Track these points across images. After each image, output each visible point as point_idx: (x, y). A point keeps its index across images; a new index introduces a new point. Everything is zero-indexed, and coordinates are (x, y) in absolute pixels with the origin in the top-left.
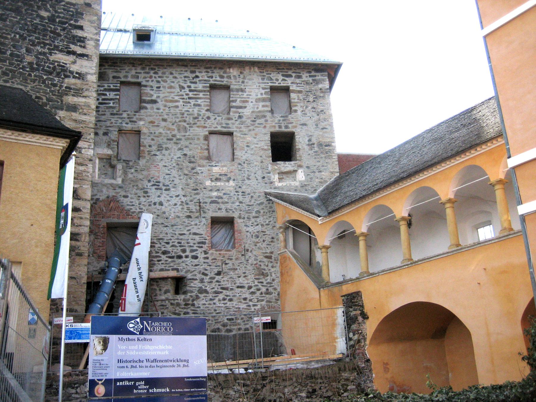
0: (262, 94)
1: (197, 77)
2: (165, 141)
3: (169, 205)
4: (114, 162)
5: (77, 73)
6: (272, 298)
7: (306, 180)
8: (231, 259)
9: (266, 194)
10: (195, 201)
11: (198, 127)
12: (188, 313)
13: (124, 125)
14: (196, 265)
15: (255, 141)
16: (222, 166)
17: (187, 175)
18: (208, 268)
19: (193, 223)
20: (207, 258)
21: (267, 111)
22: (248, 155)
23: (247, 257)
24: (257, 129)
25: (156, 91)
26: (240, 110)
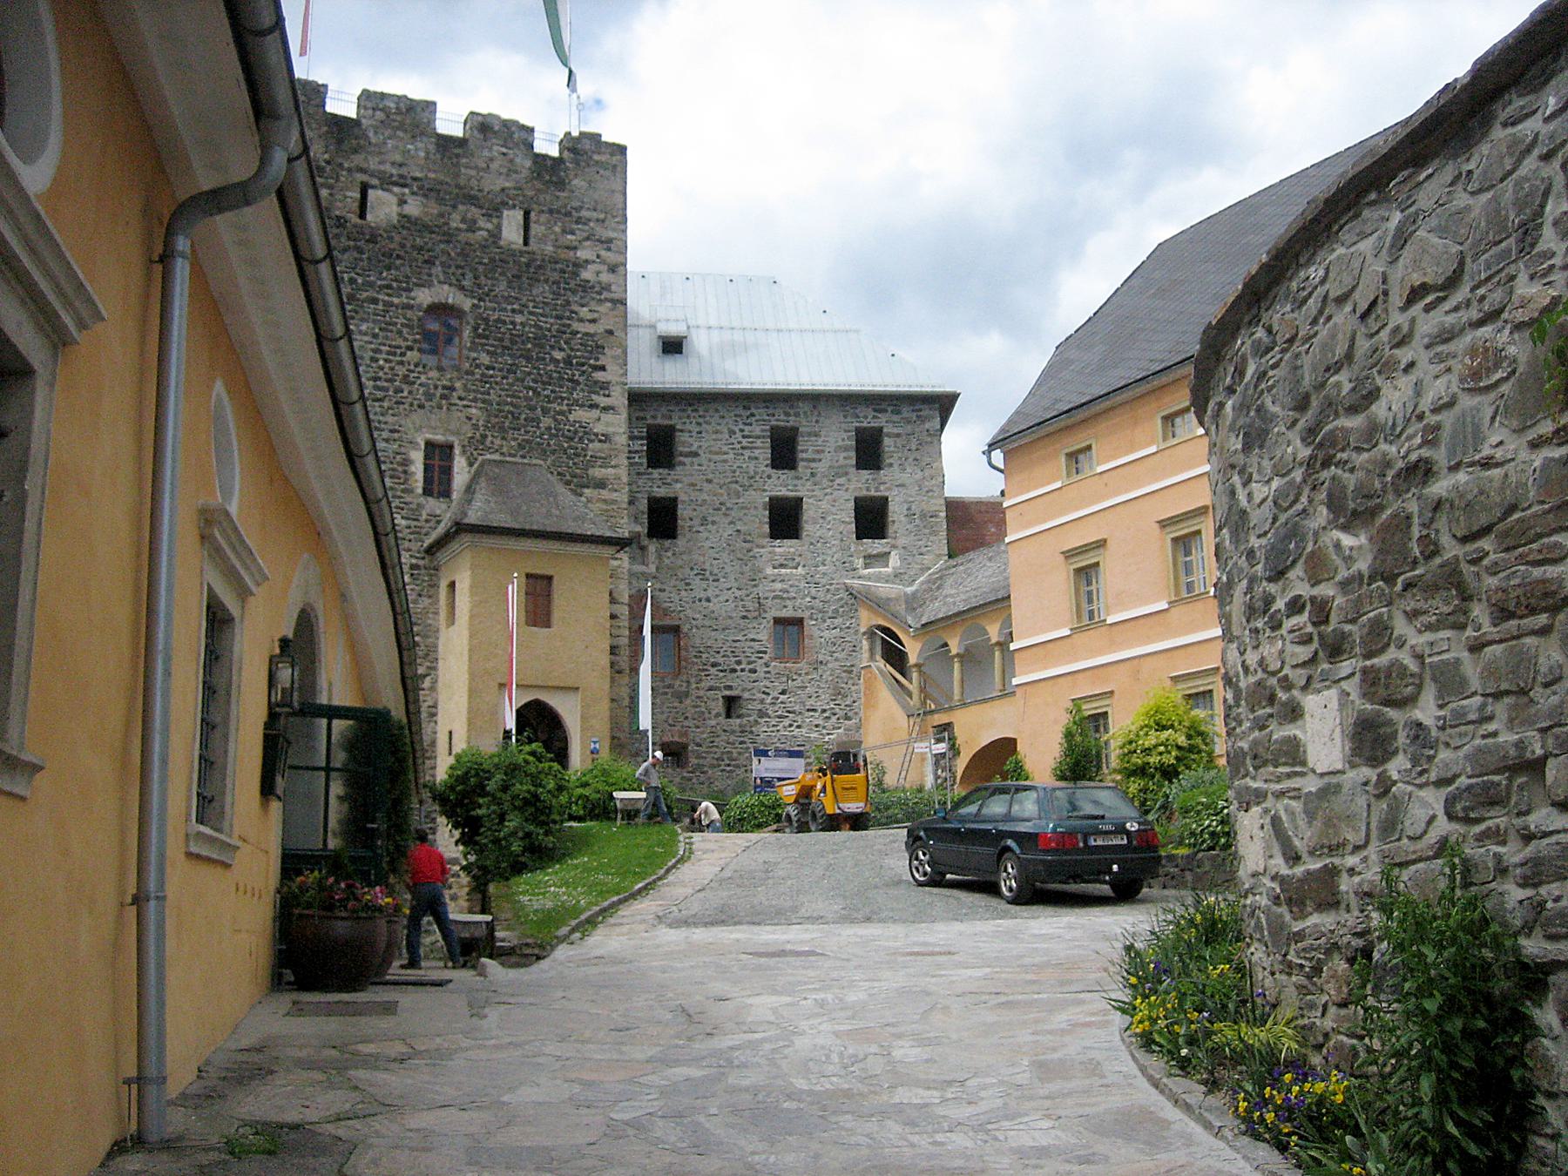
15: (834, 510)
24: (836, 493)
26: (813, 465)
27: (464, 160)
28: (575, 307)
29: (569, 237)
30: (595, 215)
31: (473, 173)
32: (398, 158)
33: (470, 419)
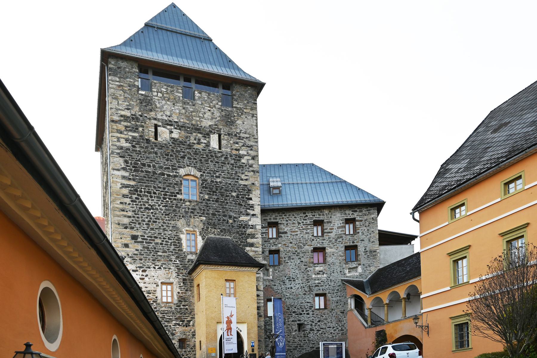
0: (340, 224)
1: (307, 216)
2: (292, 254)
3: (295, 288)
4: (268, 268)
5: (252, 226)
6: (344, 332)
7: (362, 272)
8: (325, 314)
9: (342, 280)
10: (307, 286)
11: (308, 245)
12: (305, 340)
13: (271, 247)
14: (309, 318)
16: (320, 267)
17: (303, 272)
18: (314, 319)
19: (307, 297)
20: (314, 314)
21: (343, 234)
22: (333, 260)
23: (332, 313)
24: (338, 245)
25: (286, 226)
28: (240, 175)
33: (201, 221)
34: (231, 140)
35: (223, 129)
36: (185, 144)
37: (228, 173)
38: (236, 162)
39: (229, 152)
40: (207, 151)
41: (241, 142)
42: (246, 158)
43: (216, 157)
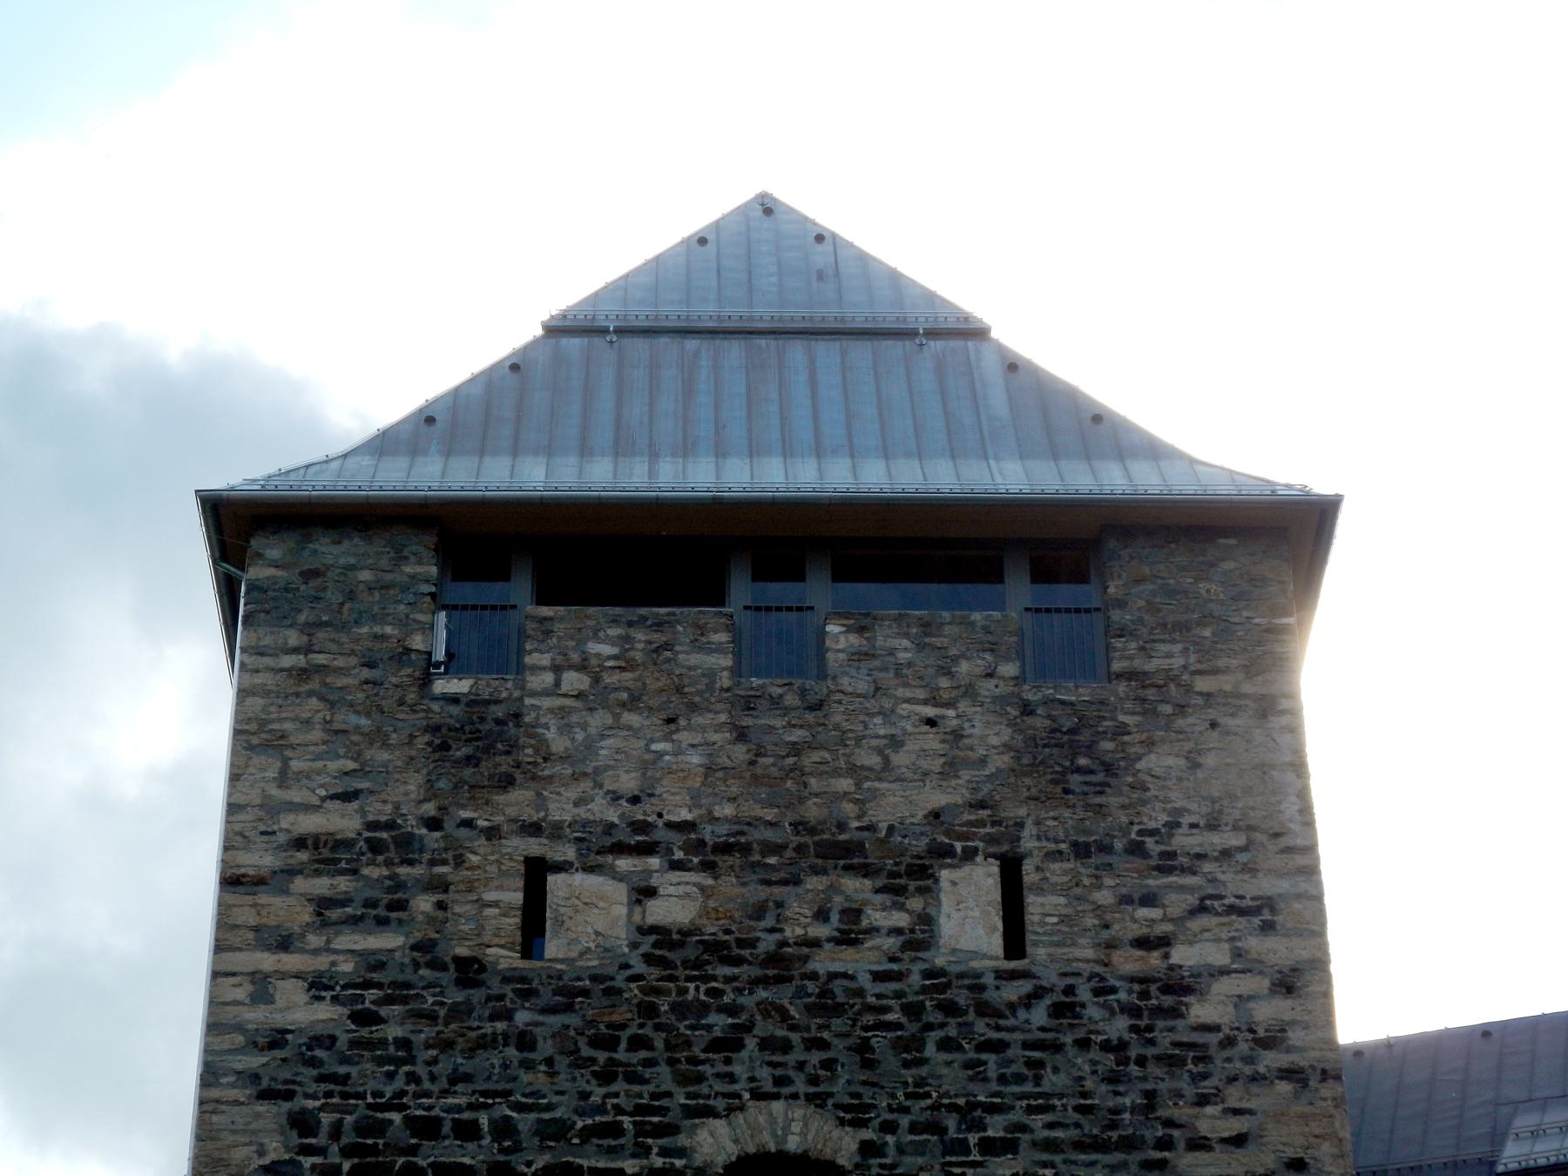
27: (816, 756)
28: (1182, 1112)
29: (1143, 912)
30: (1218, 840)
31: (845, 784)
32: (628, 782)
34: (1099, 887)
35: (1038, 823)
36: (746, 953)
37: (1079, 1109)
38: (1150, 1029)
39: (1087, 969)
40: (915, 979)
41: (1182, 889)
42: (1224, 987)
43: (984, 1009)
